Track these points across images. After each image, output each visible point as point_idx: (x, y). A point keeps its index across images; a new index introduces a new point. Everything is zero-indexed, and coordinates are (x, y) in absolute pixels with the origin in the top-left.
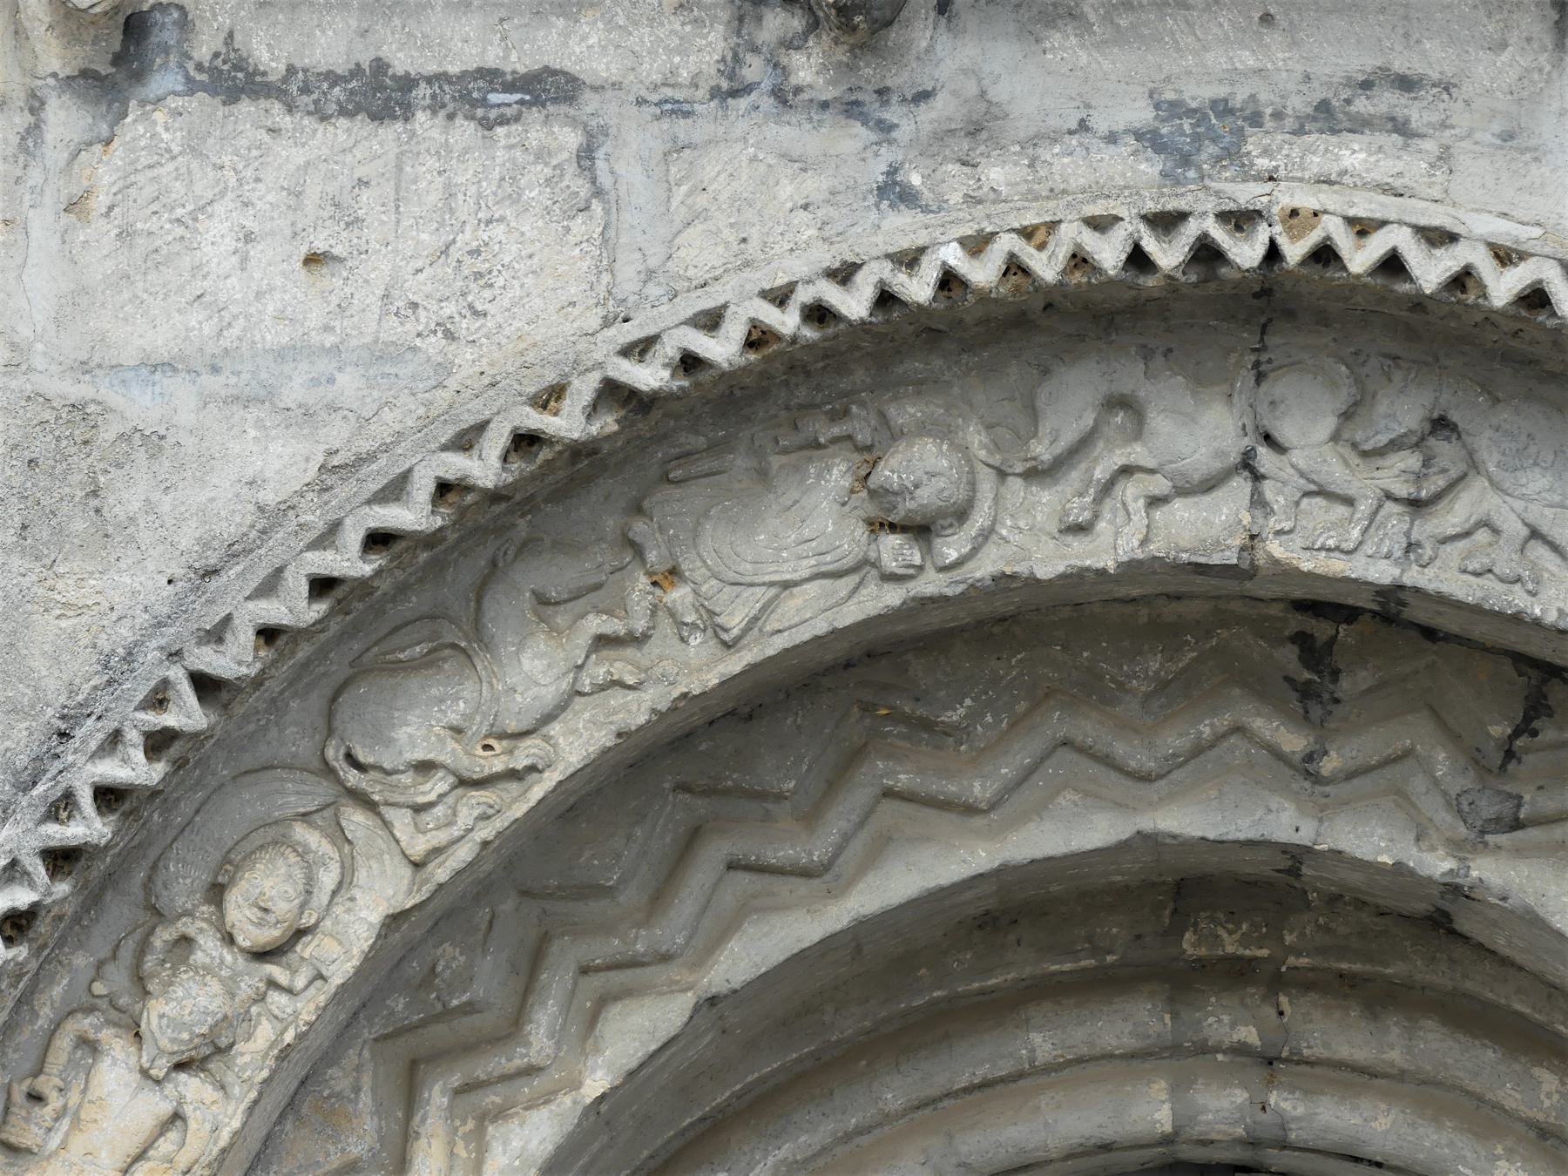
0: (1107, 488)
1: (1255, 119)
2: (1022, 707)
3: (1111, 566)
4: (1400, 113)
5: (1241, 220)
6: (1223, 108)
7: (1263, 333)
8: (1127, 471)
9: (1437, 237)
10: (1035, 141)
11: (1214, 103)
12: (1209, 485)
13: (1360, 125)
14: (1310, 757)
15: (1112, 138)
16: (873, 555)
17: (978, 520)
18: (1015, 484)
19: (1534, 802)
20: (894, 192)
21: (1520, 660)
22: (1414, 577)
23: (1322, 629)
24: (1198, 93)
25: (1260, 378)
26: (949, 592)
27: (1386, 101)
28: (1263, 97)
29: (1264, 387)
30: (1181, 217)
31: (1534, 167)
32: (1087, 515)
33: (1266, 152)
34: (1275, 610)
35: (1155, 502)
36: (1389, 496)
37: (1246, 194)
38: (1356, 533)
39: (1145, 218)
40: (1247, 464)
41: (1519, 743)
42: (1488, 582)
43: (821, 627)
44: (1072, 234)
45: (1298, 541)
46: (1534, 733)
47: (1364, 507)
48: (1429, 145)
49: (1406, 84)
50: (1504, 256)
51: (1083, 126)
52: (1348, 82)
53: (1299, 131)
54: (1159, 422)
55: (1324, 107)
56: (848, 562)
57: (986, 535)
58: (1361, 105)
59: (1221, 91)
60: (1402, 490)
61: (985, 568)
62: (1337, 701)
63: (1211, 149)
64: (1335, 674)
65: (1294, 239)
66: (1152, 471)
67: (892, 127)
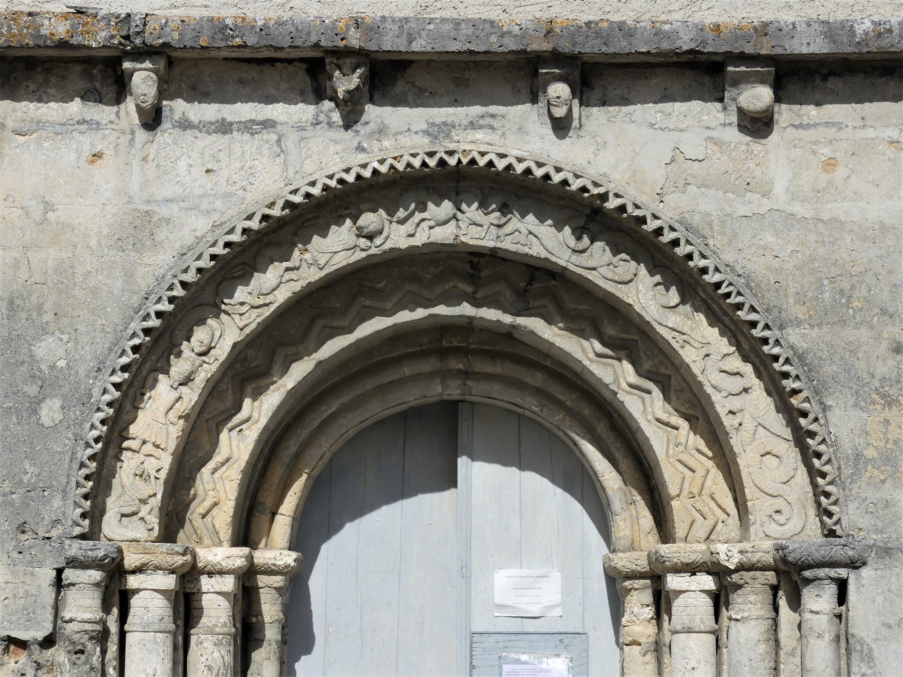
0: (418, 225)
1: (454, 127)
2: (398, 282)
3: (420, 245)
4: (491, 124)
5: (451, 153)
6: (445, 124)
7: (458, 181)
8: (423, 220)
9: (502, 156)
10: (396, 134)
11: (443, 123)
12: (445, 223)
13: (481, 127)
14: (474, 293)
15: (416, 133)
16: (358, 244)
17: (385, 234)
18: (394, 224)
19: (532, 303)
20: (360, 149)
21: (528, 266)
22: (499, 245)
23: (476, 260)
24: (438, 120)
25: (457, 194)
26: (378, 253)
27: (488, 121)
28: (455, 121)
29: (459, 196)
30: (435, 153)
31: (527, 137)
32: (413, 232)
33: (457, 135)
34: (463, 255)
35: (431, 228)
36: (492, 224)
37: (452, 146)
38: (484, 234)
39: (426, 153)
40: (454, 217)
41: (528, 288)
42: (518, 246)
43: (345, 263)
44: (407, 158)
45: (469, 236)
46: (532, 285)
47: (485, 227)
48: (499, 132)
49: (493, 116)
50: (520, 160)
51: (409, 130)
52: (478, 116)
53: (465, 129)
54: (431, 206)
55: (471, 123)
56: (351, 246)
57: (387, 238)
58: (481, 122)
59: (445, 120)
60: (495, 222)
61: (388, 246)
62: (480, 278)
63: (443, 135)
64: (480, 271)
65: (465, 157)
66: (430, 220)
67: (359, 131)
